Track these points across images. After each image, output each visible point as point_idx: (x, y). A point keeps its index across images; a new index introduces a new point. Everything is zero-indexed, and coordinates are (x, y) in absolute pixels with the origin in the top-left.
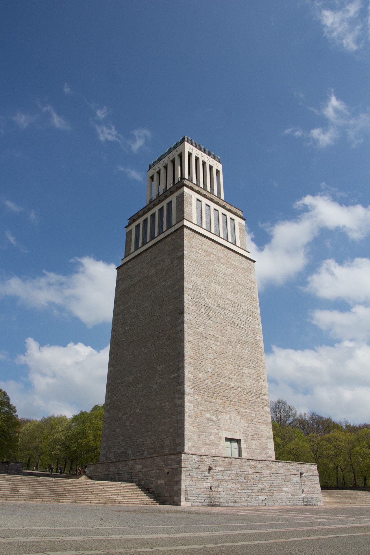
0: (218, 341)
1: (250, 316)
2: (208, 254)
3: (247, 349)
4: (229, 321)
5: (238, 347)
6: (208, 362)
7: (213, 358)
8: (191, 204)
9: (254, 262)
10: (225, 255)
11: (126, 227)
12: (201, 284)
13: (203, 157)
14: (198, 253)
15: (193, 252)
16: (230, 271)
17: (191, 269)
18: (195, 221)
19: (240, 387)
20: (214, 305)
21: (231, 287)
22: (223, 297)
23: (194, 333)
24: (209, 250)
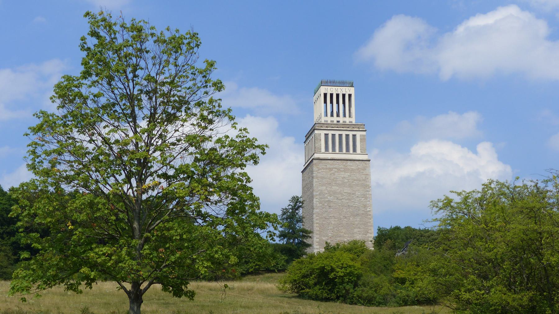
2: (331, 169)
3: (358, 219)
5: (351, 219)
8: (320, 140)
9: (369, 161)
10: (344, 165)
11: (305, 142)
16: (347, 175)
18: (323, 150)
24: (332, 167)
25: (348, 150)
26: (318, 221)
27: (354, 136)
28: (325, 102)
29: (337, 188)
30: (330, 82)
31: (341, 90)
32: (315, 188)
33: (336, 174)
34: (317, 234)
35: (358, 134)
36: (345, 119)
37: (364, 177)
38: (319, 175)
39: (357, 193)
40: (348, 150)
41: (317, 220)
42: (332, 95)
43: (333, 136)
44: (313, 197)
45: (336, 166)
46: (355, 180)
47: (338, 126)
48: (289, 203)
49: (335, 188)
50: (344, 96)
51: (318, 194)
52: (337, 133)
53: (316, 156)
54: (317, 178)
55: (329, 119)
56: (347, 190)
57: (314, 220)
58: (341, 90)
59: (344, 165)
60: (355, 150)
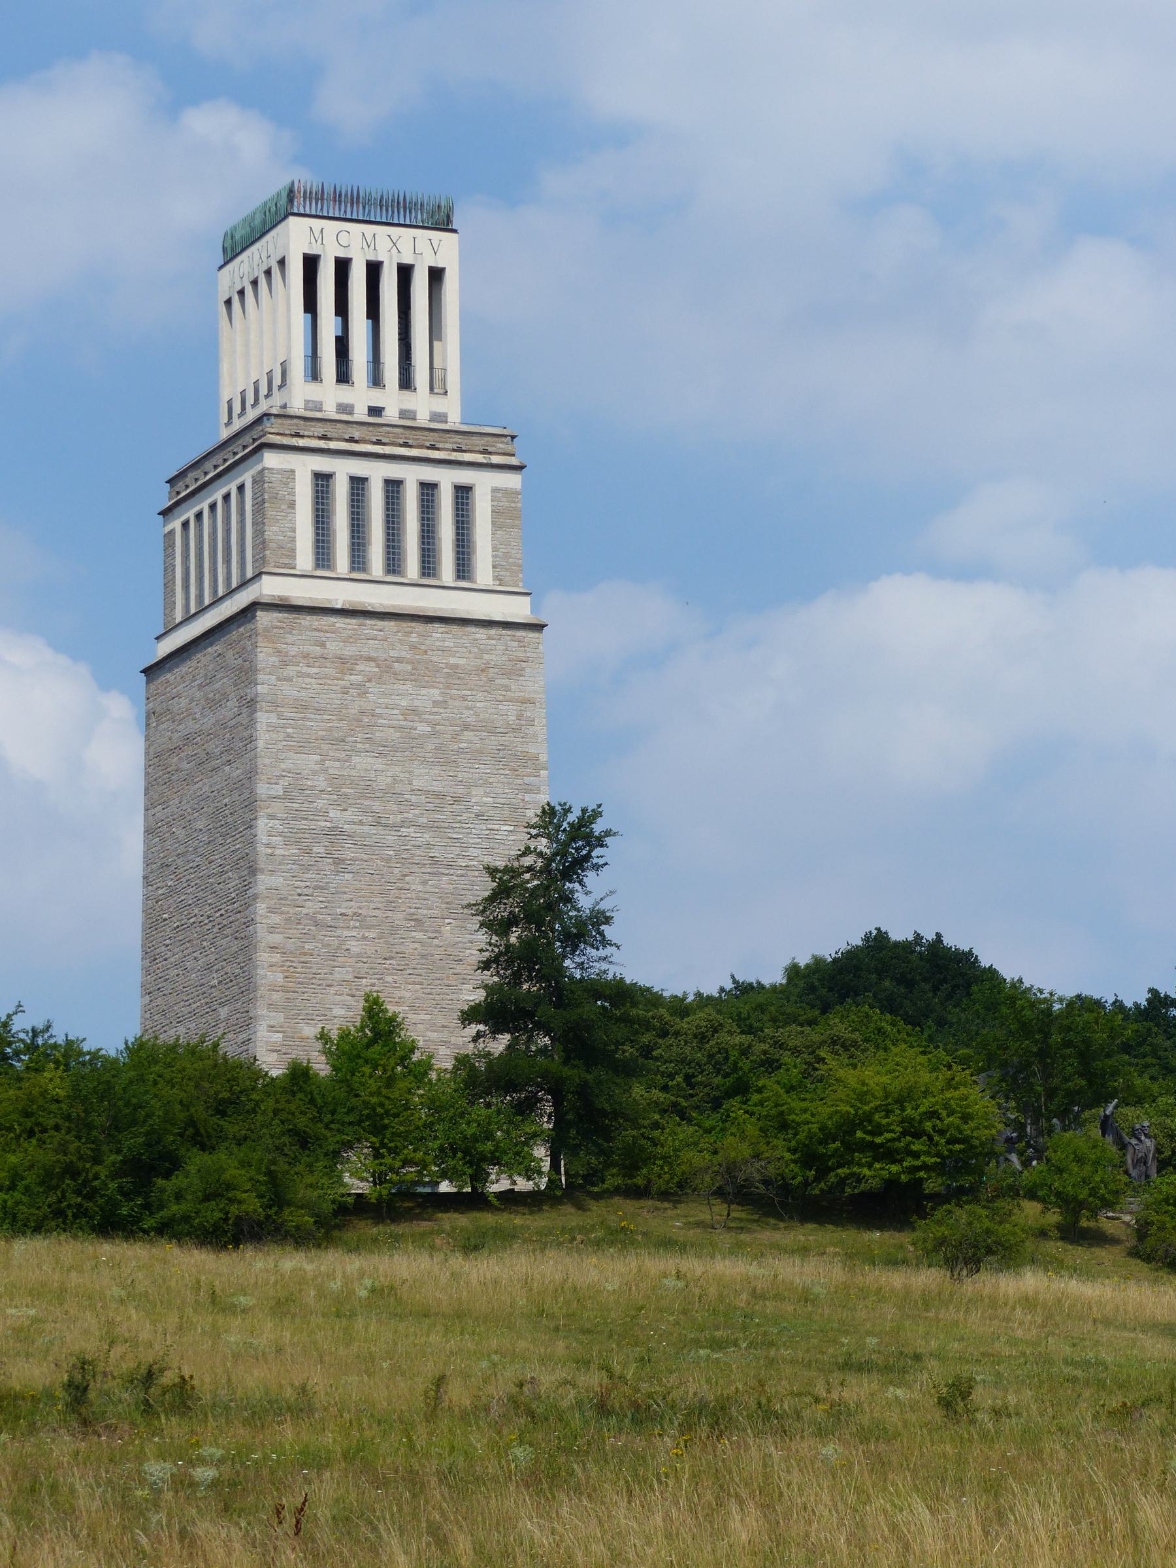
0: (368, 928)
1: (505, 821)
2: (345, 664)
4: (416, 860)
6: (332, 990)
7: (350, 977)
8: (292, 505)
9: (539, 627)
10: (413, 647)
11: (166, 513)
12: (315, 773)
13: (370, 244)
14: (309, 675)
15: (290, 680)
17: (281, 736)
18: (305, 558)
19: (446, 1043)
20: (361, 823)
21: (431, 747)
22: (399, 788)
23: (288, 920)
24: (349, 650)
25: (429, 566)
26: (277, 938)
27: (463, 492)
28: (310, 305)
29: (378, 763)
30: (337, 198)
31: (395, 245)
32: (263, 761)
33: (373, 688)
34: (271, 1006)
35: (484, 484)
36: (409, 401)
37: (512, 712)
38: (287, 691)
39: (479, 797)
40: (429, 566)
41: (272, 929)
42: (342, 267)
43: (358, 484)
44: (251, 804)
45: (373, 648)
46: (466, 727)
47: (373, 434)
48: (520, 839)
49: (364, 763)
50: (405, 273)
51: (278, 790)
52: (377, 473)
53: (270, 588)
54: (275, 705)
55: (329, 395)
56: (427, 777)
57: (261, 930)
58: (395, 245)
59: (413, 647)
60: (464, 569)
